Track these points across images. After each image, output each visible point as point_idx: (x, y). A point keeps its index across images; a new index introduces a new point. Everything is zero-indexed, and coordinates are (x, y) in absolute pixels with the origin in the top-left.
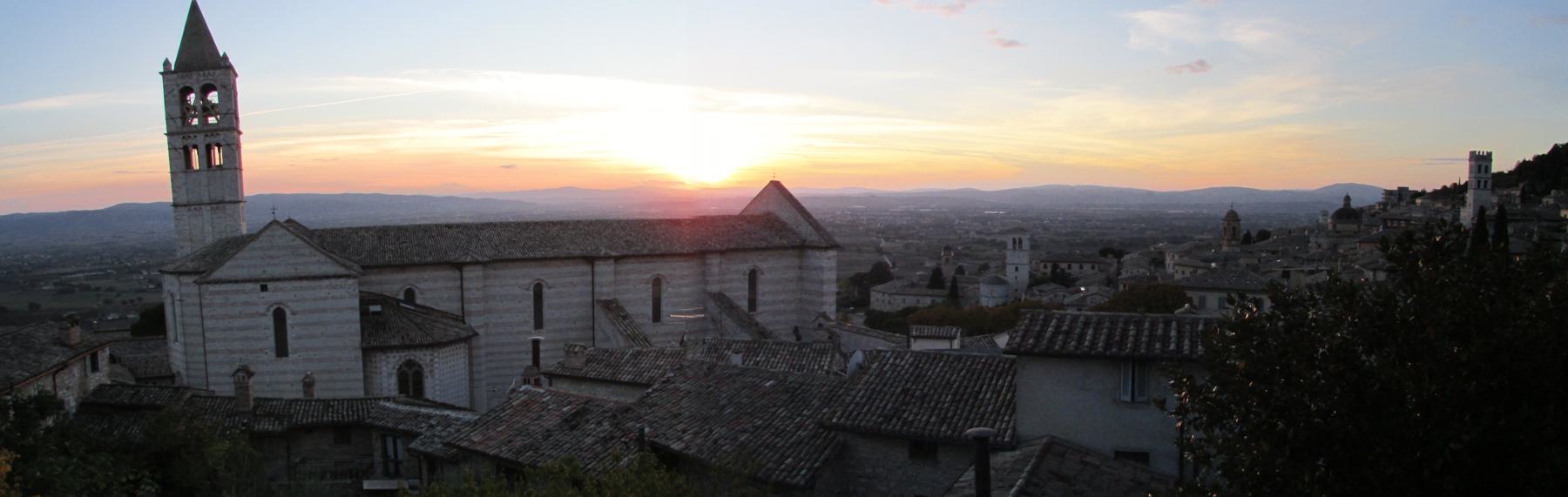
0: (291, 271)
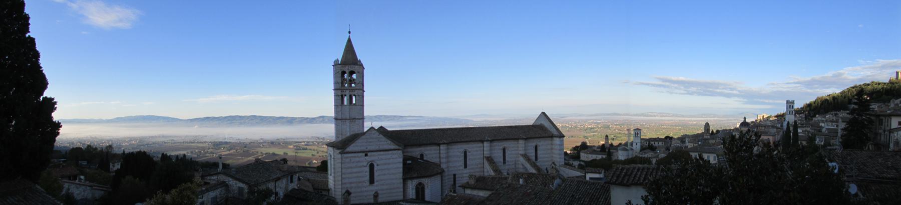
0: (377, 148)
